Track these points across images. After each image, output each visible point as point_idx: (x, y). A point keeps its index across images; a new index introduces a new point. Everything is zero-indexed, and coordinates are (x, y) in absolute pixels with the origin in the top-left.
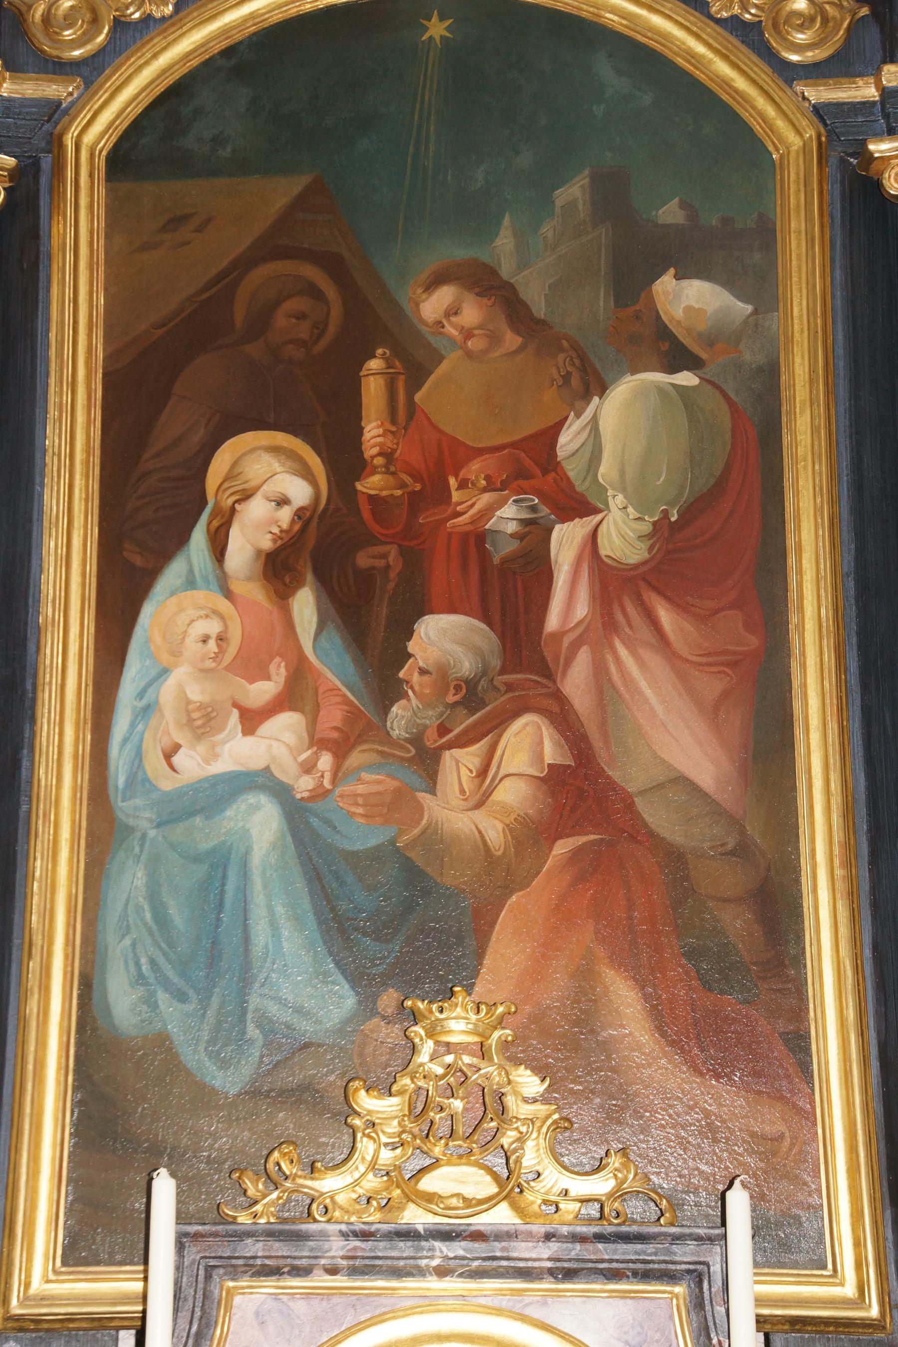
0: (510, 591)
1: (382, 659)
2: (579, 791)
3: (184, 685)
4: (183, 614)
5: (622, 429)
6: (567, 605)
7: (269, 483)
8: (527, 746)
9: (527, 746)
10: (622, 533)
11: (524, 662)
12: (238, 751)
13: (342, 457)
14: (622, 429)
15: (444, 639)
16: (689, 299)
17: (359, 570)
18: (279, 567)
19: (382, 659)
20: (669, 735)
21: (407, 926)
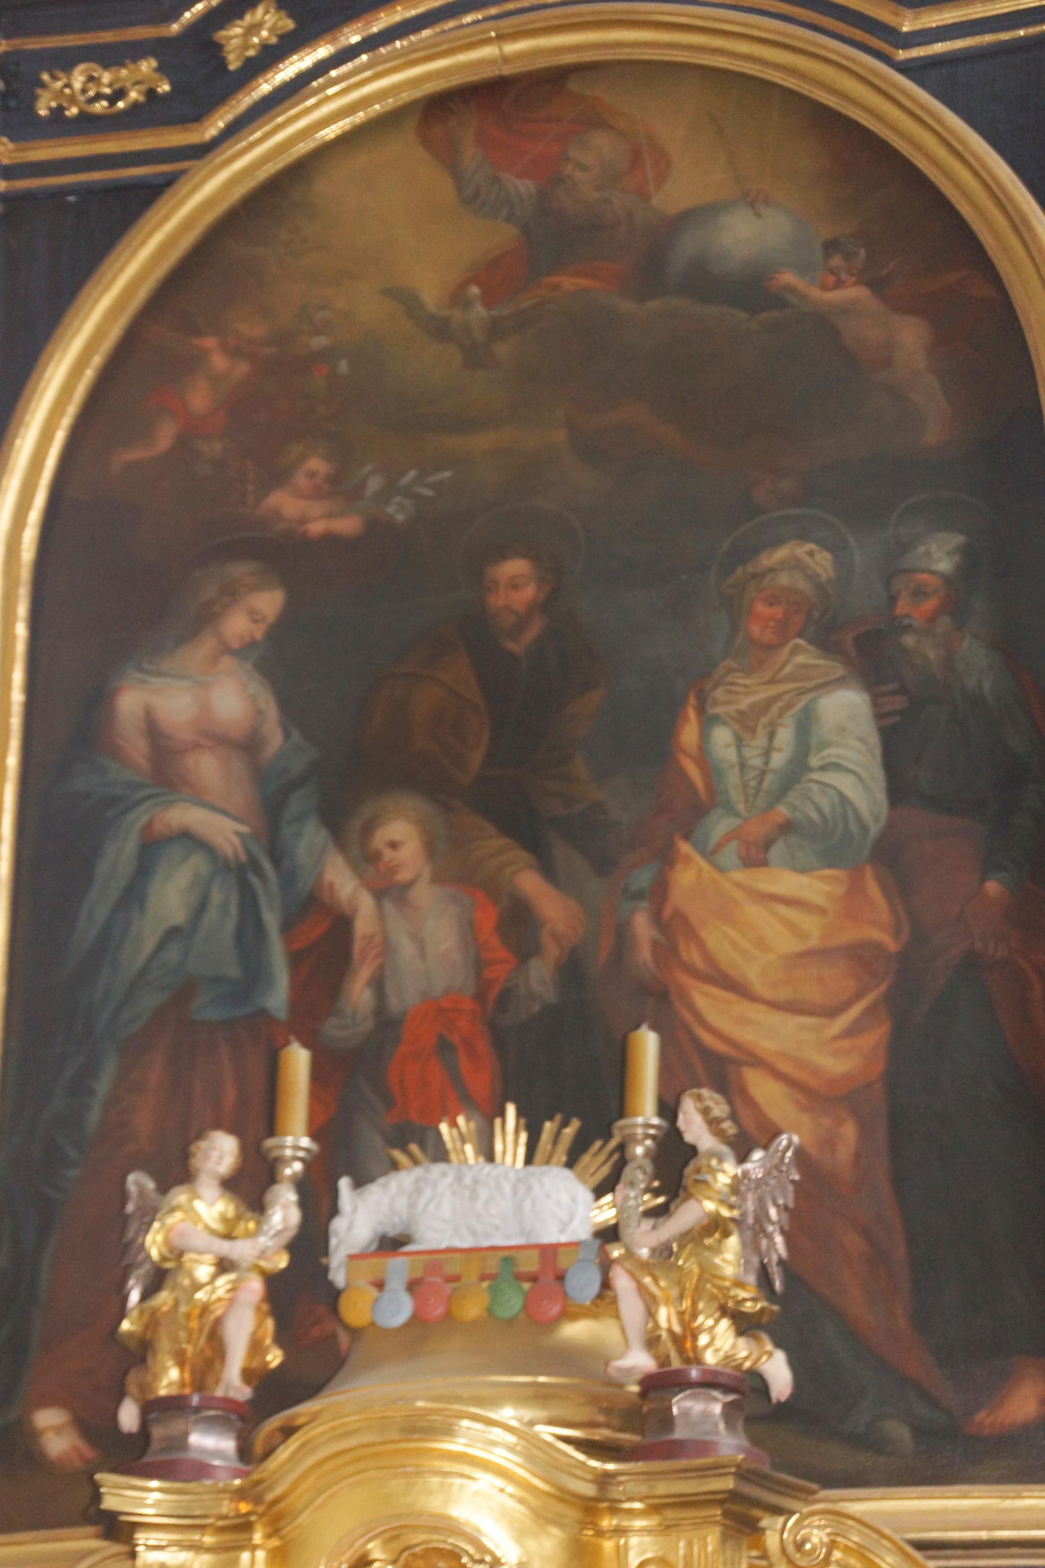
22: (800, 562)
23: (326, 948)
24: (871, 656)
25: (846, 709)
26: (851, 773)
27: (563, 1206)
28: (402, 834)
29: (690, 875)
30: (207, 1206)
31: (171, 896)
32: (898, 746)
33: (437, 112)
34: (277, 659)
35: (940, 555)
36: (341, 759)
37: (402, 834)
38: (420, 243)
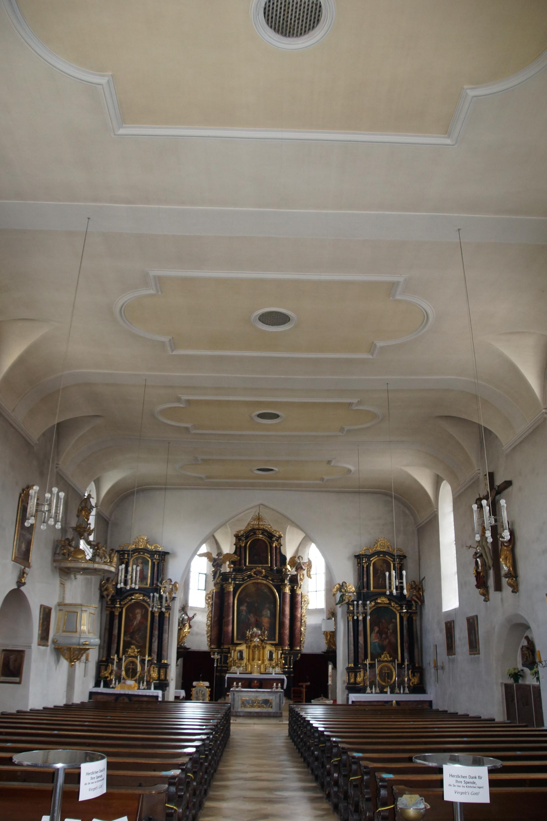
0: (387, 633)
1: (381, 637)
2: (390, 643)
3: (373, 638)
4: (373, 635)
5: (391, 626)
6: (389, 634)
7: (376, 629)
8: (387, 640)
9: (387, 640)
10: (391, 631)
11: (387, 637)
12: (376, 641)
13: (379, 628)
14: (391, 626)
15: (384, 636)
16: (394, 620)
17: (380, 633)
18: (377, 632)
19: (381, 637)
20: (393, 640)
21: (383, 649)
22: (267, 605)
23: (249, 619)
24: (270, 610)
25: (269, 612)
26: (269, 614)
27: (260, 632)
28: (252, 615)
29: (263, 618)
30: (248, 632)
31: (242, 617)
32: (271, 613)
33: (253, 583)
34: (247, 606)
35: (272, 606)
36: (249, 611)
37: (252, 615)
38: (252, 589)
